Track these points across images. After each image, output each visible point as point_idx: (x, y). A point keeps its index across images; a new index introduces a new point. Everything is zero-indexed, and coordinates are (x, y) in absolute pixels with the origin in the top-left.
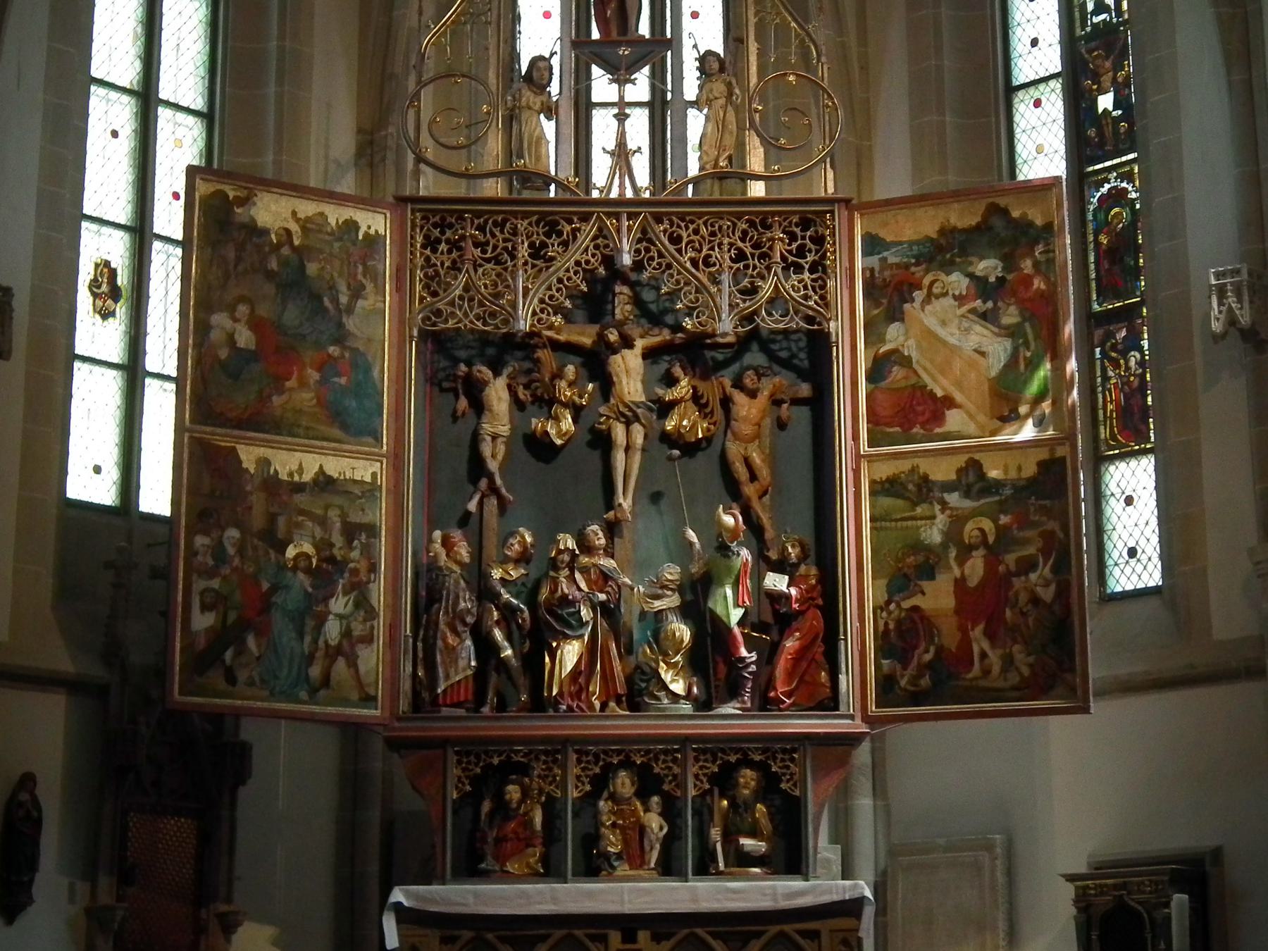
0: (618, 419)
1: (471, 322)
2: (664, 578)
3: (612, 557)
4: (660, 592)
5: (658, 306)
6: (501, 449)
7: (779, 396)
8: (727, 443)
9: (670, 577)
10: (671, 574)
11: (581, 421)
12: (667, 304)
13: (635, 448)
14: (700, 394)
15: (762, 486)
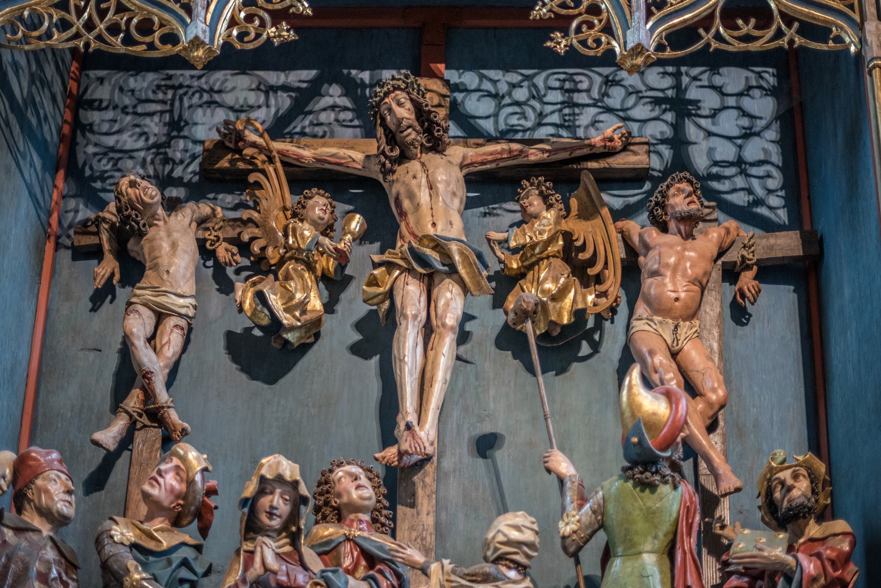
0: (410, 271)
1: (99, 38)
2: (501, 538)
3: (394, 536)
4: (489, 568)
5: (496, 122)
6: (172, 340)
7: (733, 256)
8: (635, 323)
9: (515, 535)
10: (517, 528)
11: (339, 307)
12: (514, 120)
13: (444, 325)
14: (578, 244)
15: (710, 404)
